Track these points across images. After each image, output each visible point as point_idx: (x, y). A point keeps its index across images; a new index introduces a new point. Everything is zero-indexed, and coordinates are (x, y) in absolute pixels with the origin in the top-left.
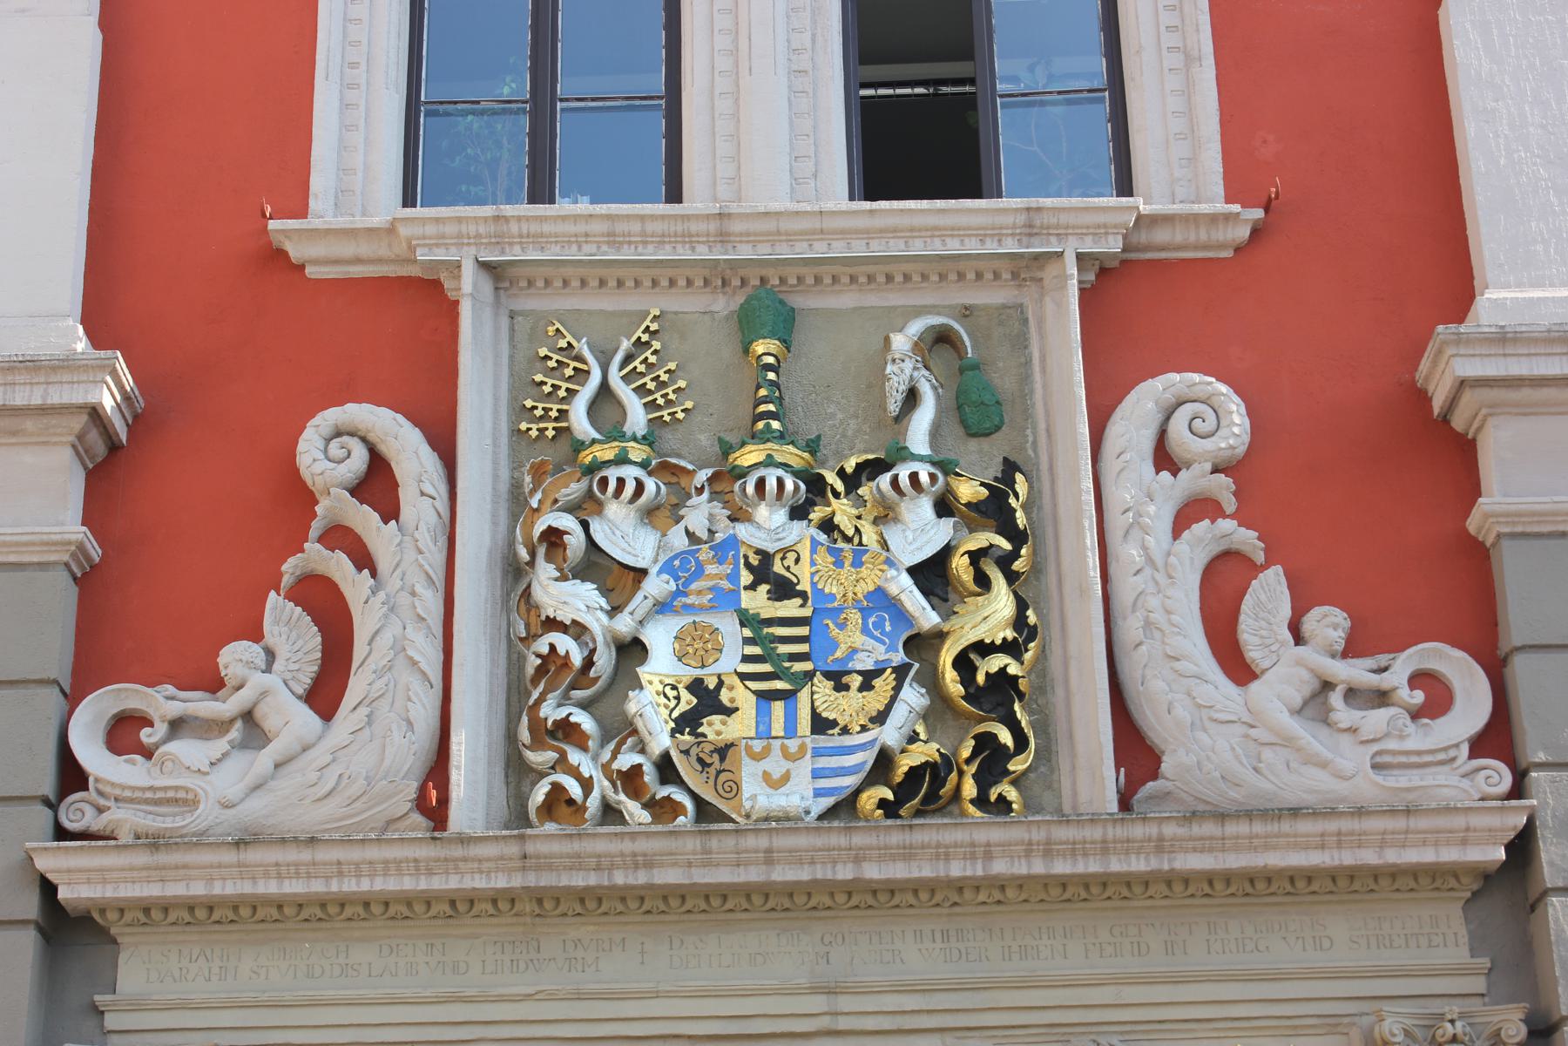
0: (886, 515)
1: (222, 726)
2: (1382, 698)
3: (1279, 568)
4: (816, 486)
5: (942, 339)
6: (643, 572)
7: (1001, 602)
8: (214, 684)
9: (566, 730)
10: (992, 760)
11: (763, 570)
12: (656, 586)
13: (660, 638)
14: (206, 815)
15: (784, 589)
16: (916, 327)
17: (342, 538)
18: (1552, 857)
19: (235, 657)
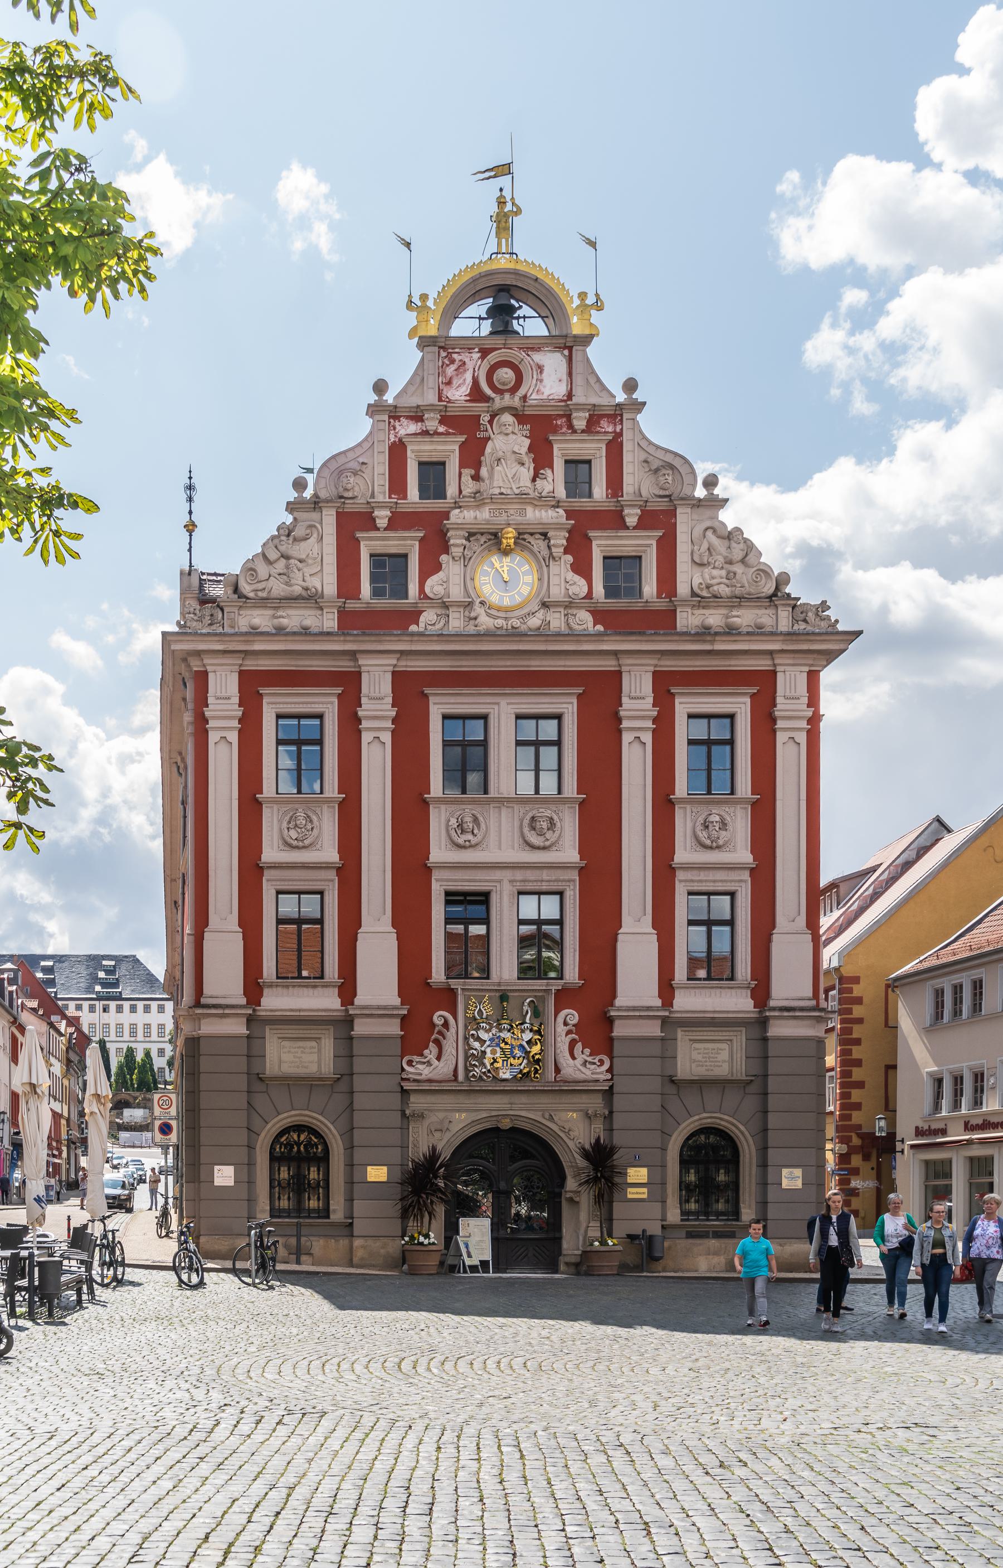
0: (523, 1031)
1: (424, 1063)
2: (594, 1064)
3: (580, 1044)
4: (512, 1026)
5: (532, 1001)
6: (485, 1041)
7: (539, 1046)
8: (422, 1055)
9: (475, 1065)
10: (536, 1071)
11: (504, 1041)
12: (488, 1043)
13: (488, 1050)
14: (423, 1077)
15: (506, 1043)
16: (528, 1001)
17: (440, 1033)
18: (615, 1089)
19: (426, 1052)
